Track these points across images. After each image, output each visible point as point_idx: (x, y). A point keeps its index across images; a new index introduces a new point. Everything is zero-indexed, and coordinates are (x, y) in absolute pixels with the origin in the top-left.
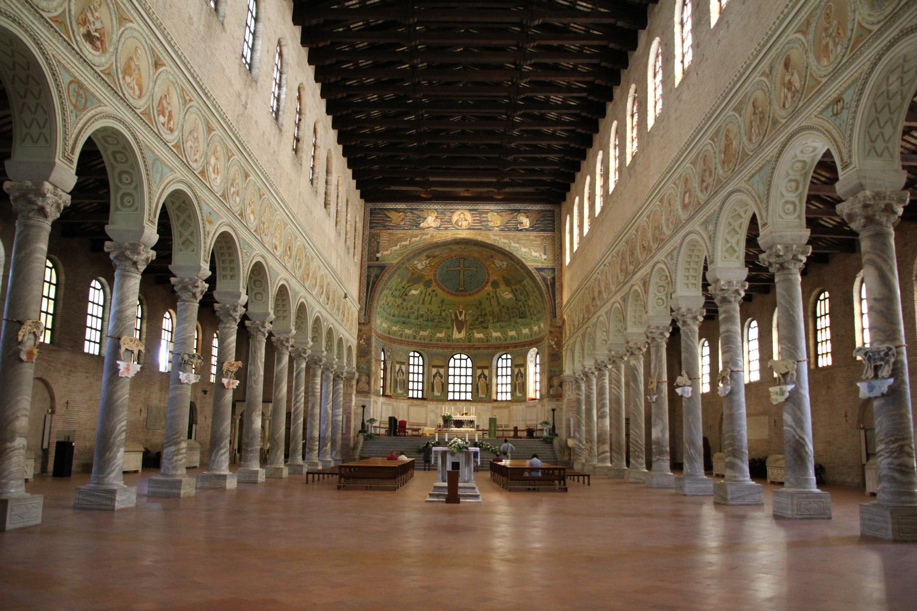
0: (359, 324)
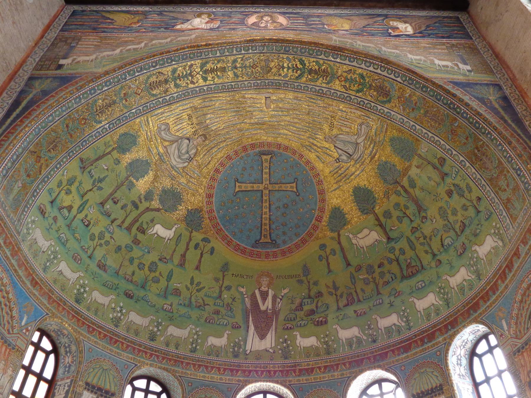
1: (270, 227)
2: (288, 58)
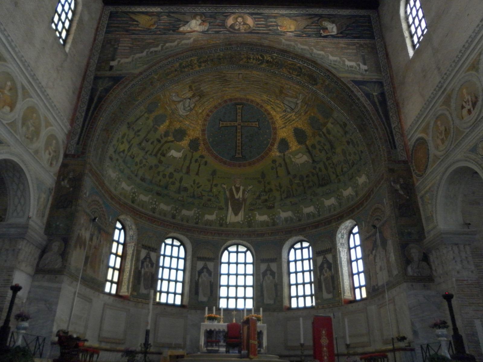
0: (66, 156)
1: (241, 148)
2: (253, 54)
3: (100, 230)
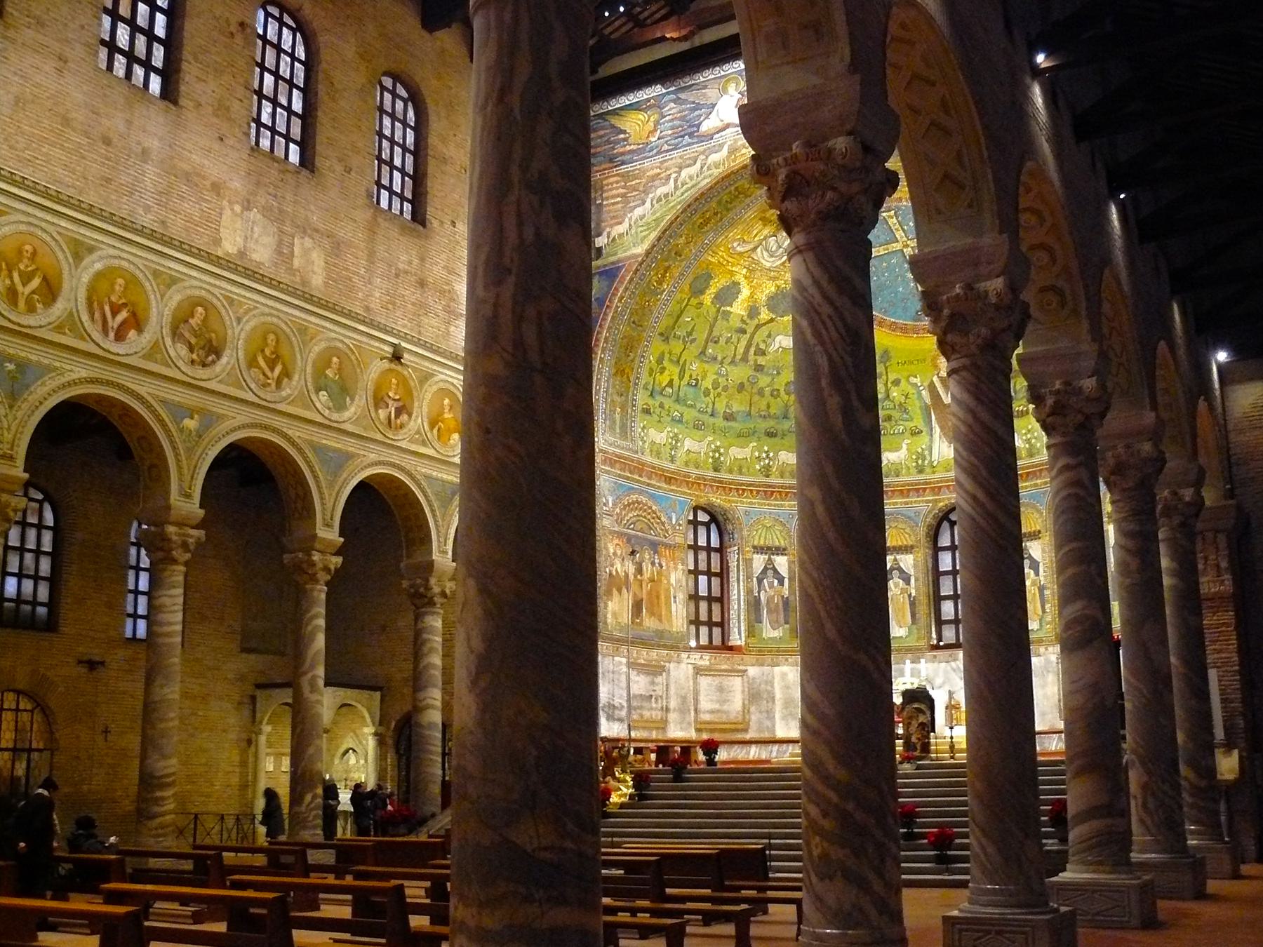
3: (654, 546)
